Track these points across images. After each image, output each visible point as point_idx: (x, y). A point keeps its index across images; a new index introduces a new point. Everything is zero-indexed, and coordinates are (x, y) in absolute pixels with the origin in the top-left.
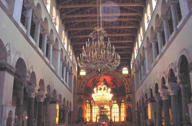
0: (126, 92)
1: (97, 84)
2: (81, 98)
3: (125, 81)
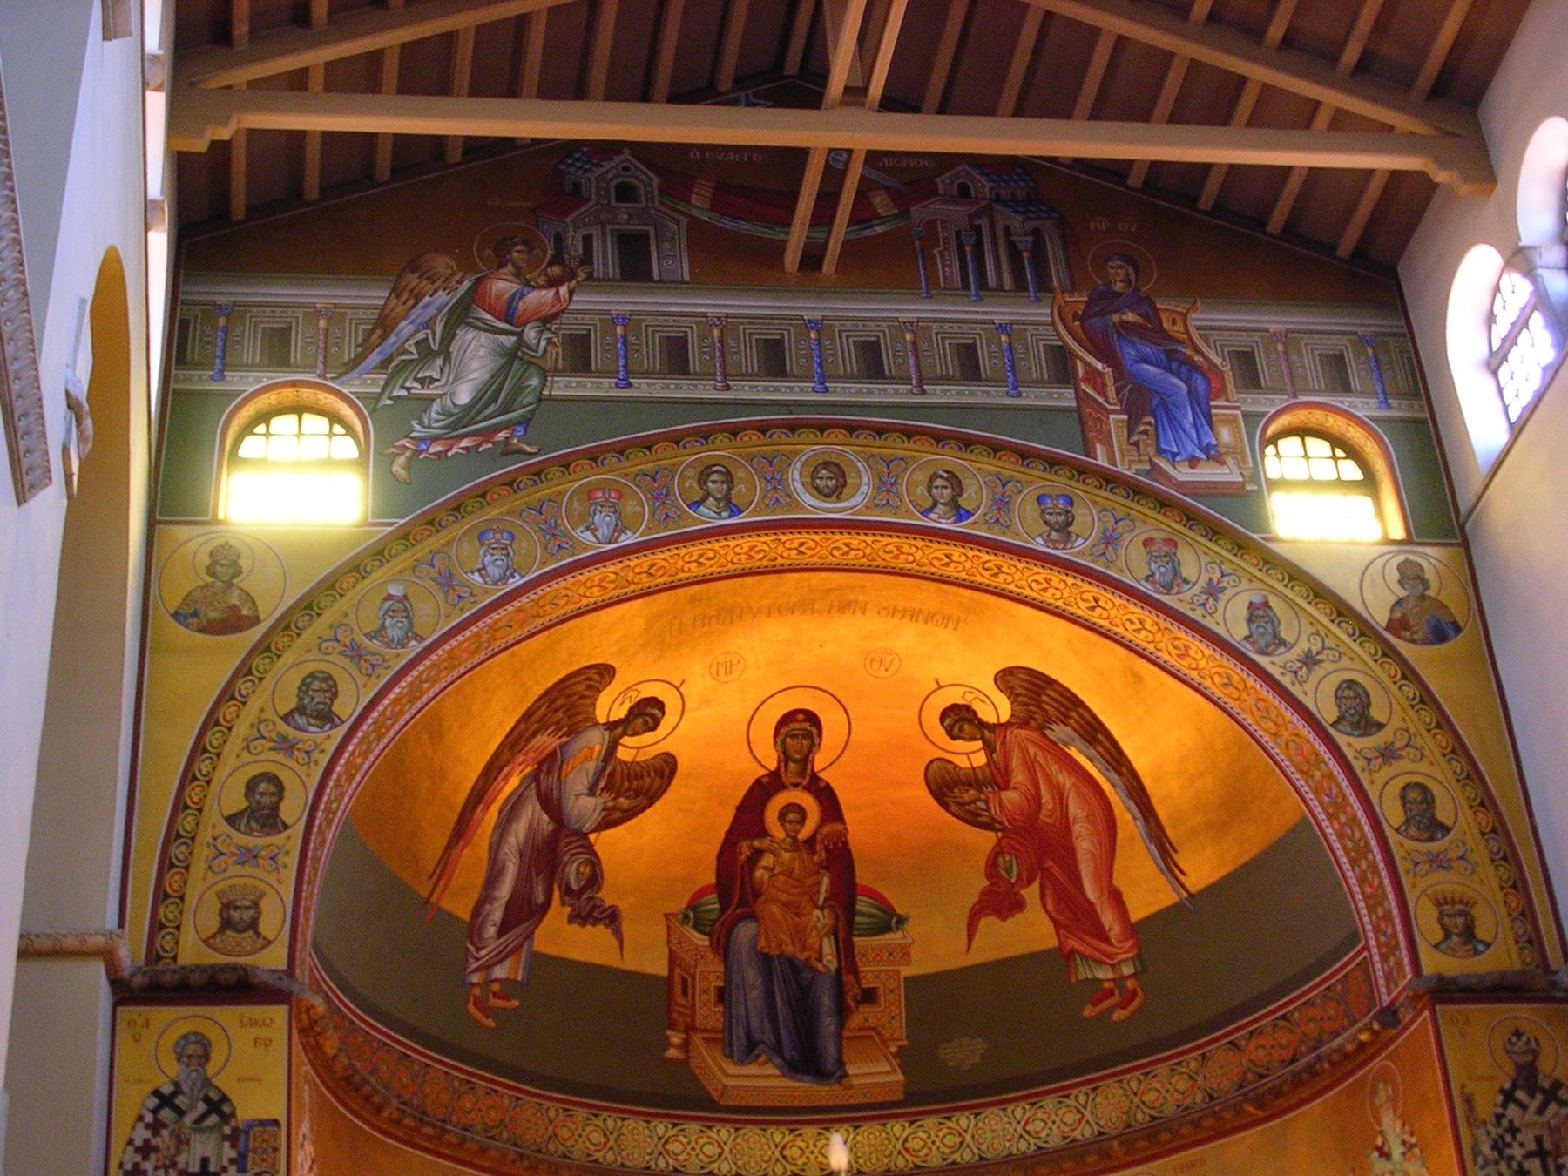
0: (1434, 963)
1: (604, 842)
2: (218, 1105)
3: (1365, 724)
